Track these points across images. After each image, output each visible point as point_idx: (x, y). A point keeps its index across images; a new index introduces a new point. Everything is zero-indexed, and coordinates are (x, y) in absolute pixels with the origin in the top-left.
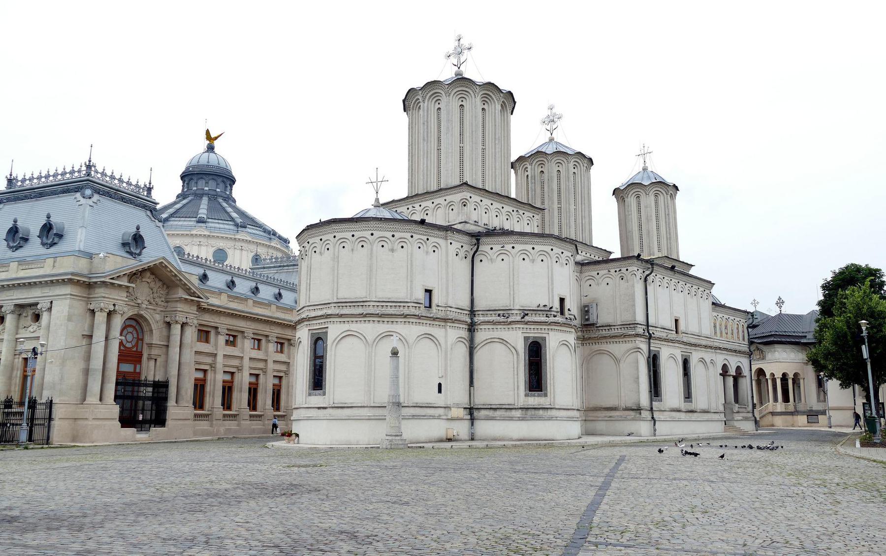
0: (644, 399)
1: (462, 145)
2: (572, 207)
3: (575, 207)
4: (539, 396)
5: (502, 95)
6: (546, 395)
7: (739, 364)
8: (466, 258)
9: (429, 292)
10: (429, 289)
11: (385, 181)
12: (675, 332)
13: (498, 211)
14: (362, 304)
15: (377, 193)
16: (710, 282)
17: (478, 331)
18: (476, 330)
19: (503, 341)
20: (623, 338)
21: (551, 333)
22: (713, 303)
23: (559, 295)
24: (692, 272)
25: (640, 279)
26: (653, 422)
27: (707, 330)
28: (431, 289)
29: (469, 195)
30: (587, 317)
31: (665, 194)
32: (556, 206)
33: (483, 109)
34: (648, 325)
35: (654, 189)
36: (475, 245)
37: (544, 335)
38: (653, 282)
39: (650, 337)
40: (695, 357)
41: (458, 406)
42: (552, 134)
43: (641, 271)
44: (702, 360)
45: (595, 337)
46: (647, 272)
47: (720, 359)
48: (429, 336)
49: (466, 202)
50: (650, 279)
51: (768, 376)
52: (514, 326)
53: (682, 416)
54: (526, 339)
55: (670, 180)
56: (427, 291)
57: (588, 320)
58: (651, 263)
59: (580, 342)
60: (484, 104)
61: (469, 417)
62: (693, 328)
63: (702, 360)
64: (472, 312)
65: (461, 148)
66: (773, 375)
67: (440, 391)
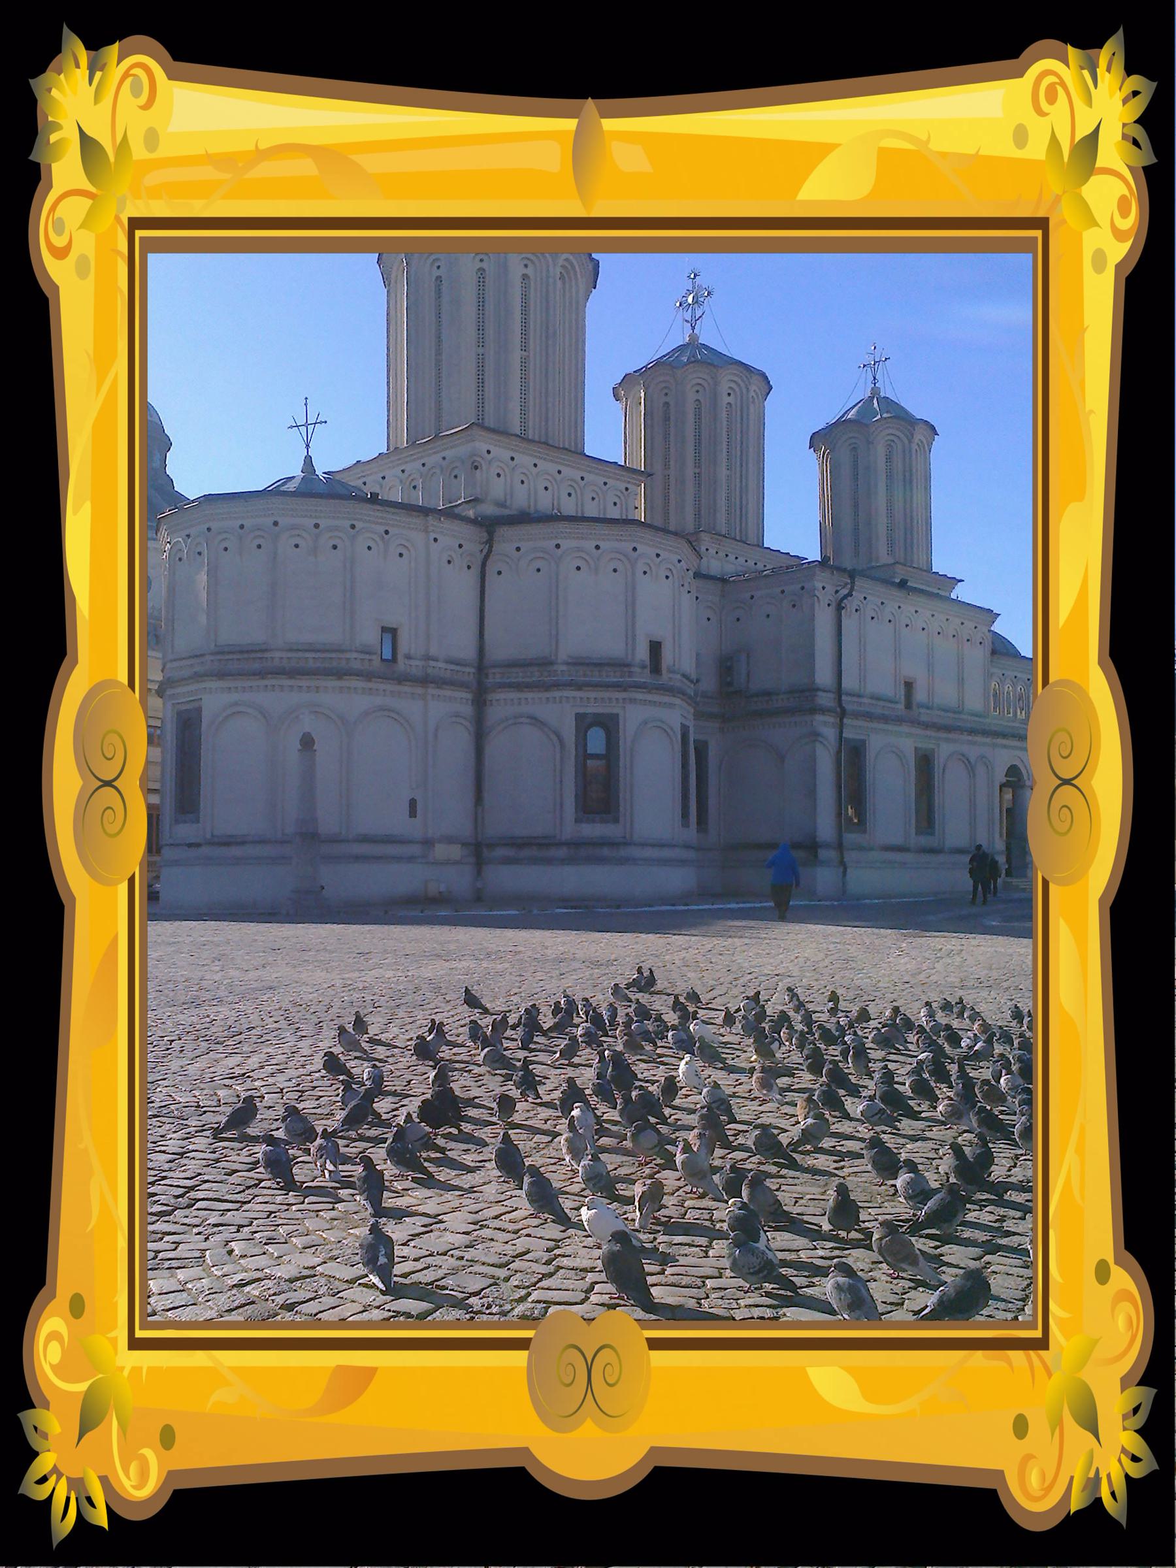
0: (825, 828)
1: (481, 350)
2: (723, 472)
3: (728, 472)
4: (603, 821)
6: (616, 820)
8: (469, 567)
9: (391, 632)
10: (390, 626)
11: (321, 423)
12: (901, 706)
13: (549, 478)
14: (259, 655)
15: (308, 446)
17: (491, 705)
18: (488, 703)
19: (535, 720)
22: (994, 652)
24: (959, 593)
25: (829, 605)
26: (841, 869)
28: (395, 626)
30: (729, 679)
31: (906, 442)
32: (690, 471)
33: (525, 277)
34: (839, 691)
36: (486, 543)
37: (615, 711)
38: (856, 610)
39: (843, 714)
40: (944, 750)
41: (449, 840)
42: (693, 328)
43: (830, 589)
46: (845, 591)
49: (479, 462)
50: (851, 604)
52: (557, 694)
53: (909, 857)
54: (579, 717)
55: (918, 411)
56: (384, 630)
57: (730, 684)
58: (852, 575)
60: (526, 266)
61: (472, 860)
62: (946, 693)
64: (481, 665)
65: (481, 357)
67: (413, 813)
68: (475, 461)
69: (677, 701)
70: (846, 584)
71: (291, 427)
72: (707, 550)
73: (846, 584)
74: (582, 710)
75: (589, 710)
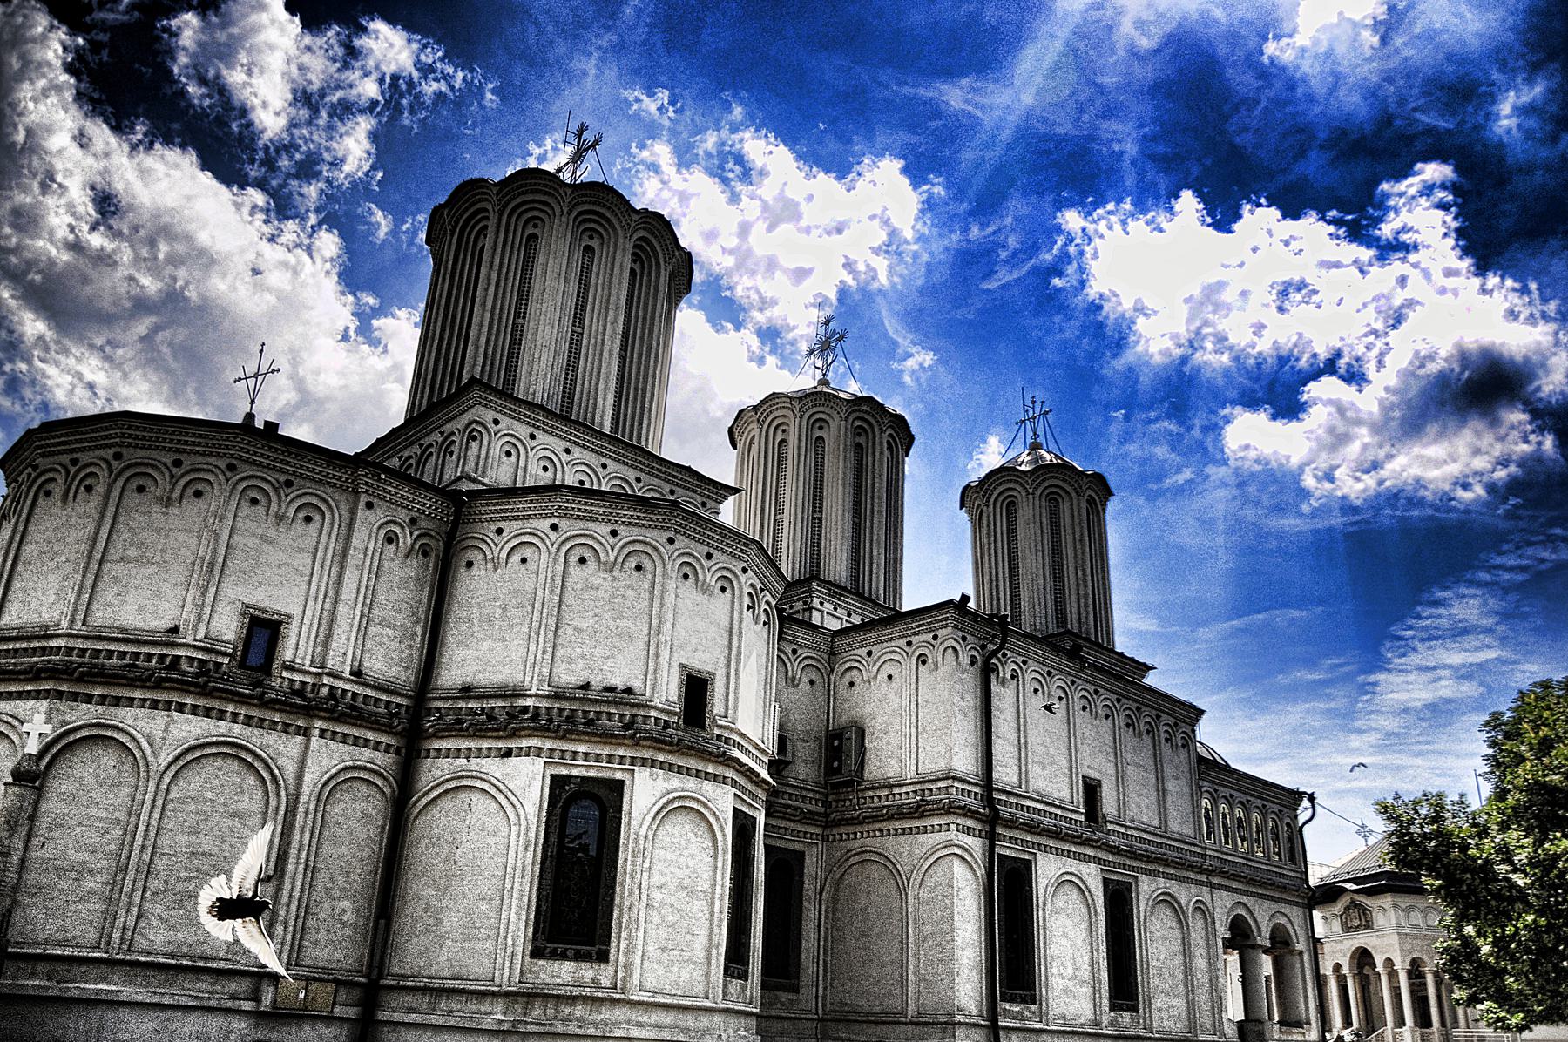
4: (579, 957)
5: (636, 217)
7: (1282, 920)
16: (1192, 706)
20: (919, 818)
21: (642, 774)
23: (682, 667)
24: (1151, 680)
27: (1180, 824)
29: (489, 416)
31: (1074, 495)
35: (1046, 484)
37: (618, 776)
38: (1013, 677)
40: (1146, 888)
44: (1169, 901)
45: (853, 818)
46: (991, 647)
47: (1223, 904)
48: (232, 751)
51: (1380, 967)
54: (558, 782)
59: (819, 831)
63: (1169, 901)
66: (1389, 962)
68: (474, 430)
69: (730, 773)
70: (995, 636)
71: (240, 379)
72: (822, 604)
73: (995, 636)
74: (564, 771)
75: (575, 772)
